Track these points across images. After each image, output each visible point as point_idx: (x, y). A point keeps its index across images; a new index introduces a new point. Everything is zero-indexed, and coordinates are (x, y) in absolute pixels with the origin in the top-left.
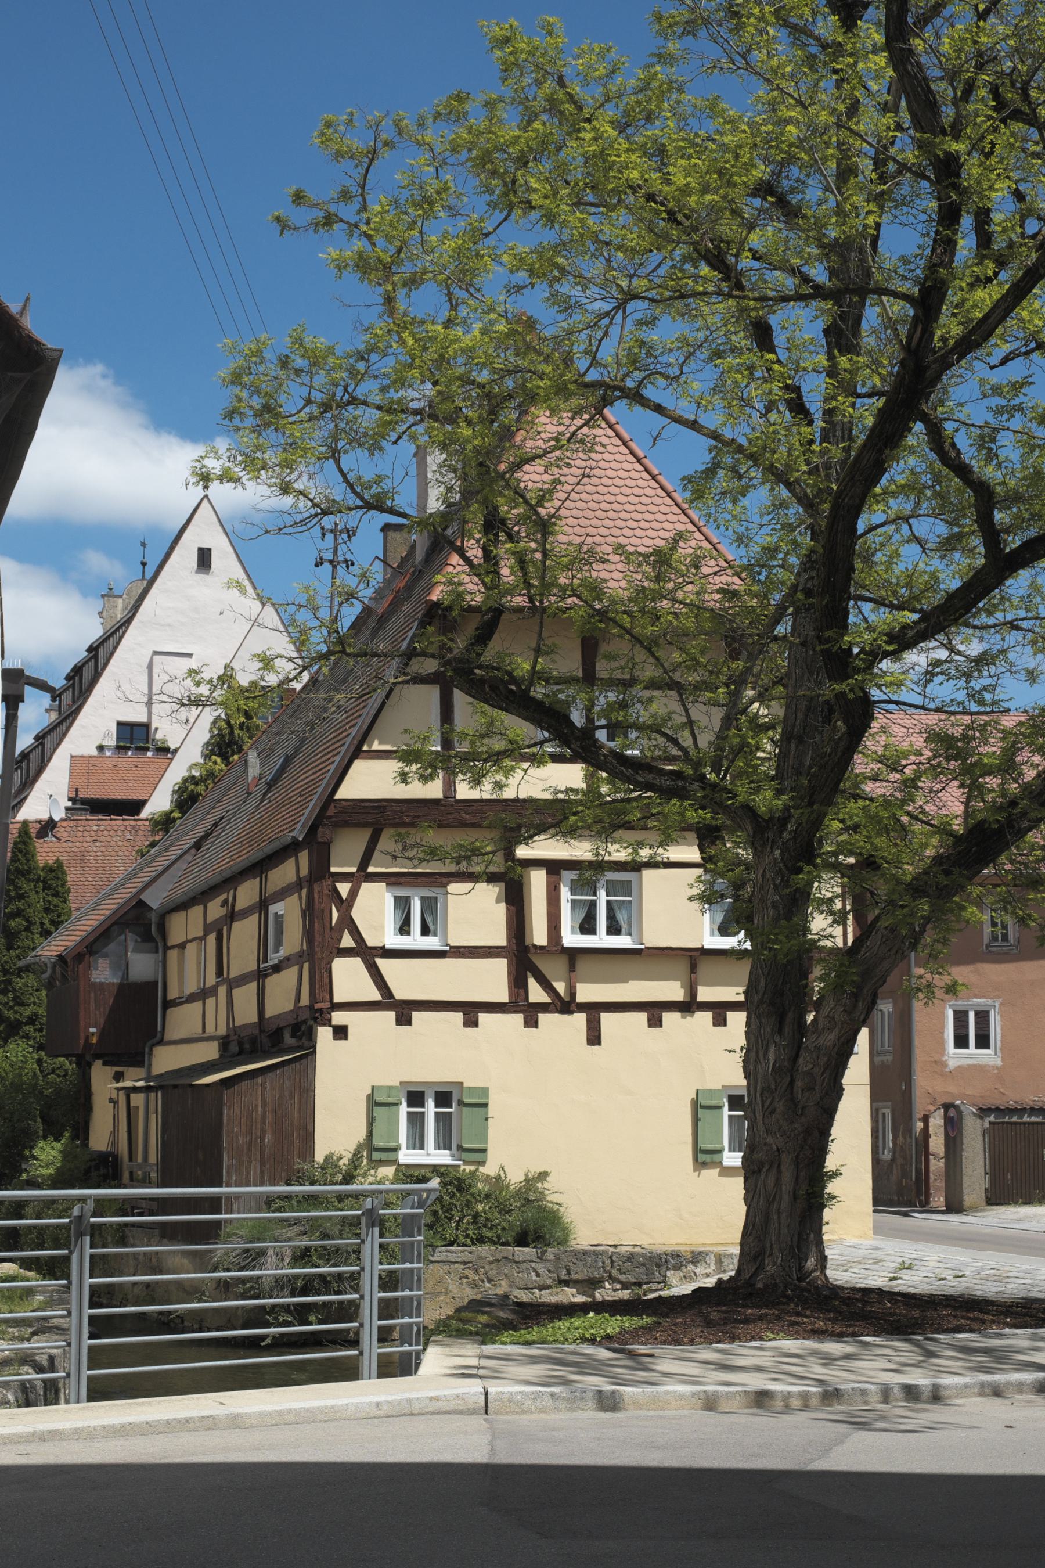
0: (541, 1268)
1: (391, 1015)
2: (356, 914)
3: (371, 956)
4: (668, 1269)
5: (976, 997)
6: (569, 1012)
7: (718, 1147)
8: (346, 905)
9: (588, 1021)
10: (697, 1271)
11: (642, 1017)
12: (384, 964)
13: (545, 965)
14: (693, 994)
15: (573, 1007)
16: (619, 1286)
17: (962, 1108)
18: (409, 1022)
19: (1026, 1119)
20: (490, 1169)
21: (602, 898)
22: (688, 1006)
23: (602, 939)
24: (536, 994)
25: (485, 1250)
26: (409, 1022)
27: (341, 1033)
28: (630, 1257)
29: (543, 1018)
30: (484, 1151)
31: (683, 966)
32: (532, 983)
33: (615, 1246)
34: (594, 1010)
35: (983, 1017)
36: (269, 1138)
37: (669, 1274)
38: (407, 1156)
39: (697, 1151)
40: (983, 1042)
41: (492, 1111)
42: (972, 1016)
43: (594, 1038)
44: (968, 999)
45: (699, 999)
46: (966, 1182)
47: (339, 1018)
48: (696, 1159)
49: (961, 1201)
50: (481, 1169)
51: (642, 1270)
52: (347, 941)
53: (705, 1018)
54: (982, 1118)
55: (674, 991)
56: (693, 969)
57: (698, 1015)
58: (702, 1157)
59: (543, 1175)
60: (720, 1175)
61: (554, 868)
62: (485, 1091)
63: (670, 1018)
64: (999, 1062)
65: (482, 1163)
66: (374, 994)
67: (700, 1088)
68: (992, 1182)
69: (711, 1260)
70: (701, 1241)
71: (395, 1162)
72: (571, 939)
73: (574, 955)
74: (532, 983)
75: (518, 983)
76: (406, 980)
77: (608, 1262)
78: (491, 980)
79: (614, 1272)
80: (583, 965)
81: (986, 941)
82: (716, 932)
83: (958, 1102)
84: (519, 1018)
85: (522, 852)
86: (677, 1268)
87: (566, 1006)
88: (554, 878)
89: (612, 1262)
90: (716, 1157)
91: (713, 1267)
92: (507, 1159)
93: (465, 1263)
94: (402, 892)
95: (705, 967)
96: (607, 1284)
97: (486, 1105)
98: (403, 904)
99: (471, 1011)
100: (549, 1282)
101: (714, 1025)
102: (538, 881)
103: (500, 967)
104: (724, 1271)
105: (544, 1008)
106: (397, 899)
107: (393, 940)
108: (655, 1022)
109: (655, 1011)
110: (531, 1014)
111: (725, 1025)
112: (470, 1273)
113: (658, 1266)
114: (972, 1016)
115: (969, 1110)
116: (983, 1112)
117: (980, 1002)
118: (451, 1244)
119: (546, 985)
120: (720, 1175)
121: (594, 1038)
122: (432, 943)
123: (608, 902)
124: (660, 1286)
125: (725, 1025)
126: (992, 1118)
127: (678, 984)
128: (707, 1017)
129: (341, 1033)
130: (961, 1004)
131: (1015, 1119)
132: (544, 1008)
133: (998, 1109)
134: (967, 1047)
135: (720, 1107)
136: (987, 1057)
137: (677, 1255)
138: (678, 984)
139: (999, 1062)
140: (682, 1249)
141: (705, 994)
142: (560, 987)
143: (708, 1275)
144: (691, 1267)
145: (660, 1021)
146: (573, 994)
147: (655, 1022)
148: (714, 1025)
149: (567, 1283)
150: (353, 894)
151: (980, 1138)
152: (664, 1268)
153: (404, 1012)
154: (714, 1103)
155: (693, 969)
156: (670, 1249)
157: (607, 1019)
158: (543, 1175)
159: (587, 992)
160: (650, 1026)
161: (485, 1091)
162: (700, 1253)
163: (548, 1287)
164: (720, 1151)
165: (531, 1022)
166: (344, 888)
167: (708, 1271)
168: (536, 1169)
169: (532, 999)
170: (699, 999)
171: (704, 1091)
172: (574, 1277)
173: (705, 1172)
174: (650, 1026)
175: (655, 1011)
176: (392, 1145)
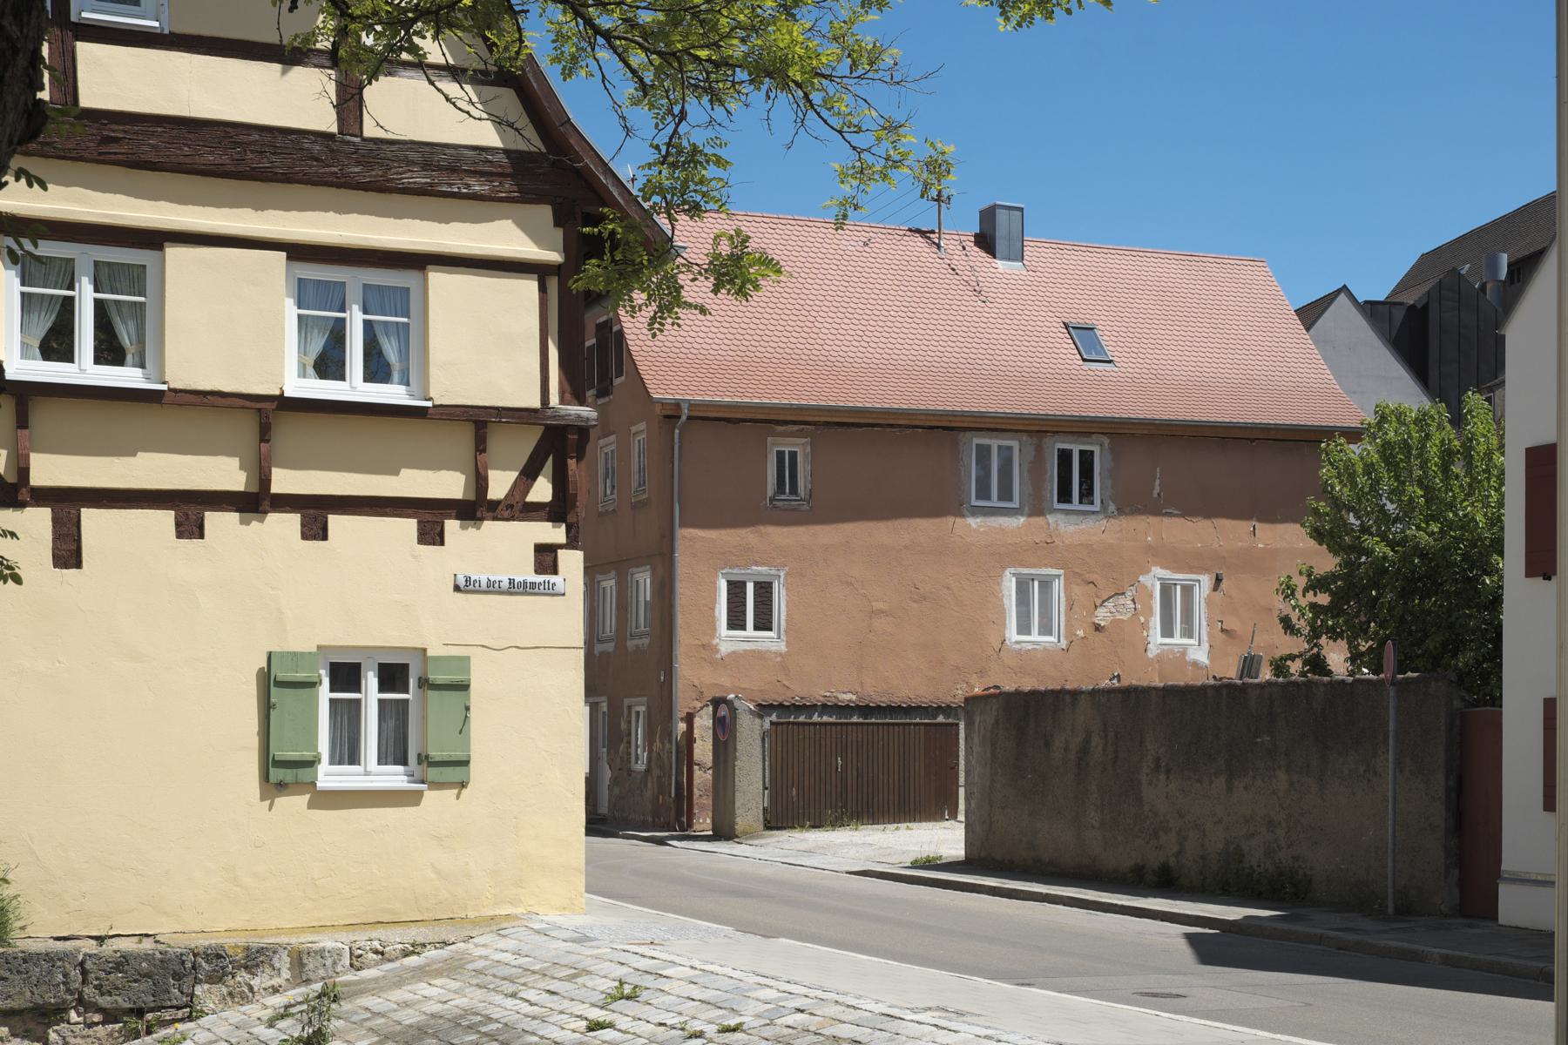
4: (197, 981)
5: (756, 563)
6: (20, 505)
7: (307, 755)
10: (255, 982)
11: (165, 519)
14: (265, 481)
16: (97, 1018)
17: (737, 704)
19: (816, 718)
21: (86, 296)
22: (254, 502)
28: (122, 962)
31: (246, 427)
33: (100, 939)
35: (764, 590)
37: (198, 990)
40: (763, 623)
42: (750, 588)
44: (746, 566)
45: (275, 489)
46: (739, 800)
48: (265, 776)
49: (732, 824)
51: (146, 985)
53: (288, 524)
54: (761, 717)
55: (228, 474)
56: (265, 433)
57: (273, 518)
58: (276, 774)
60: (311, 806)
63: (219, 522)
64: (782, 647)
67: (275, 648)
68: (774, 799)
69: (283, 962)
70: (274, 924)
77: (76, 974)
79: (89, 991)
81: (770, 493)
82: (310, 370)
83: (731, 696)
86: (216, 978)
89: (84, 973)
90: (303, 774)
91: (286, 974)
95: (288, 431)
96: (73, 1015)
101: (305, 537)
104: (308, 981)
108: (190, 528)
109: (190, 510)
111: (325, 538)
113: (178, 976)
114: (750, 588)
115: (745, 706)
116: (764, 709)
117: (762, 570)
120: (311, 806)
123: (99, 304)
124: (180, 1014)
125: (325, 538)
126: (774, 718)
127: (234, 462)
130: (737, 574)
131: (802, 719)
133: (781, 706)
134: (743, 627)
135: (313, 685)
136: (769, 641)
137: (216, 955)
138: (234, 462)
139: (782, 647)
140: (228, 941)
141: (284, 481)
143: (275, 990)
144: (242, 976)
145: (201, 527)
147: (190, 528)
148: (305, 537)
151: (759, 742)
152: (189, 980)
154: (301, 676)
155: (265, 433)
156: (202, 942)
157: (92, 520)
160: (180, 535)
162: (260, 951)
164: (311, 764)
167: (276, 982)
170: (275, 489)
171: (282, 655)
173: (283, 802)
174: (180, 535)
175: (190, 510)
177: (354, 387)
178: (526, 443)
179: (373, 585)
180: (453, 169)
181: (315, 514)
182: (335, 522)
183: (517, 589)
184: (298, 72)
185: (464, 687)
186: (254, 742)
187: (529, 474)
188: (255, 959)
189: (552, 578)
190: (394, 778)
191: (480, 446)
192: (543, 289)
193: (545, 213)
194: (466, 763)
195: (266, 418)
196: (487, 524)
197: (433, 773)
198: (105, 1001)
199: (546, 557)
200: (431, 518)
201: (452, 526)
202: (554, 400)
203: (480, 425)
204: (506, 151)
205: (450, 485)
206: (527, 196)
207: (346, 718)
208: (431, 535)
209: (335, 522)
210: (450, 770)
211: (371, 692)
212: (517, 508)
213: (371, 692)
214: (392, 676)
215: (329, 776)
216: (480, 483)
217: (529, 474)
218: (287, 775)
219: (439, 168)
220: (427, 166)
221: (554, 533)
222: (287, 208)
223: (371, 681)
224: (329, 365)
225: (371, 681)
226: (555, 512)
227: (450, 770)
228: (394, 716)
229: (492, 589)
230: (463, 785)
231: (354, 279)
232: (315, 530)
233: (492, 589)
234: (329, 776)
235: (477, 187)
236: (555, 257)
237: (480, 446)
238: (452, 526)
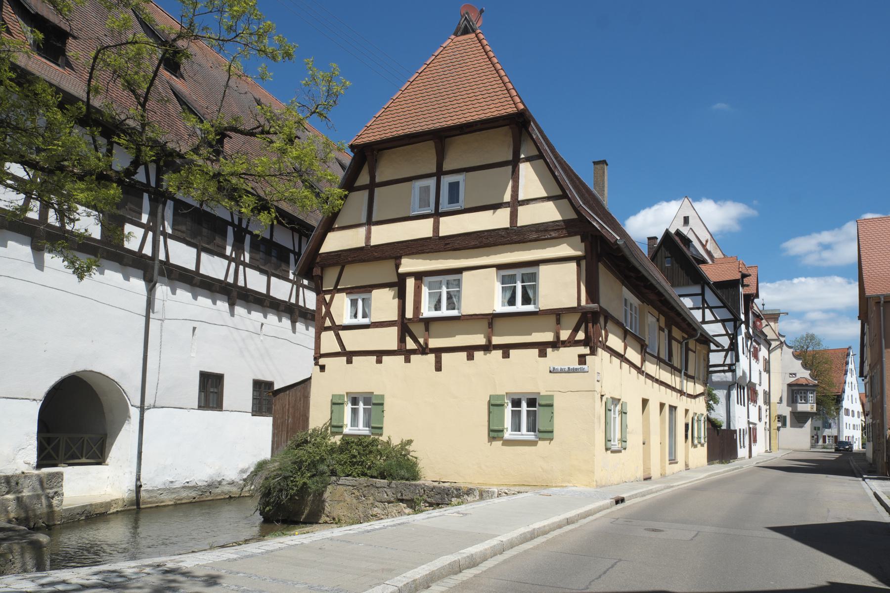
0: (388, 491)
1: (345, 359)
2: (332, 310)
3: (337, 329)
6: (427, 354)
8: (328, 305)
9: (436, 357)
10: (469, 499)
11: (464, 354)
12: (341, 333)
13: (414, 328)
14: (489, 341)
15: (427, 351)
18: (351, 363)
20: (384, 438)
22: (487, 348)
23: (444, 312)
24: (410, 344)
25: (362, 480)
26: (351, 363)
27: (322, 368)
29: (413, 357)
30: (381, 428)
32: (409, 340)
34: (438, 352)
36: (290, 420)
38: (347, 430)
39: (491, 431)
41: (386, 407)
43: (438, 368)
47: (322, 361)
50: (381, 438)
52: (328, 323)
53: (499, 353)
55: (480, 340)
57: (494, 352)
58: (492, 434)
59: (410, 442)
61: (419, 276)
62: (382, 397)
63: (478, 355)
65: (381, 435)
66: (339, 350)
69: (477, 493)
71: (341, 433)
72: (427, 312)
73: (428, 322)
74: (409, 340)
75: (402, 340)
76: (353, 340)
78: (389, 338)
80: (433, 327)
84: (402, 358)
85: (402, 270)
86: (458, 496)
87: (424, 350)
88: (419, 282)
90: (500, 434)
92: (393, 433)
93: (353, 486)
94: (354, 297)
95: (498, 324)
97: (382, 404)
98: (354, 303)
99: (379, 355)
100: (392, 499)
102: (410, 283)
103: (394, 331)
105: (413, 352)
106: (352, 300)
107: (347, 320)
108: (470, 357)
109: (470, 351)
110: (407, 354)
112: (355, 491)
113: (447, 495)
118: (348, 476)
119: (415, 340)
121: (438, 368)
122: (366, 321)
127: (482, 336)
128: (499, 353)
129: (322, 368)
132: (413, 352)
137: (458, 489)
138: (482, 336)
141: (496, 340)
142: (421, 341)
144: (466, 497)
146: (426, 344)
147: (470, 357)
149: (402, 501)
150: (332, 299)
153: (350, 356)
154: (499, 402)
157: (445, 356)
158: (410, 442)
159: (434, 343)
161: (382, 397)
162: (471, 489)
163: (392, 502)
165: (408, 360)
166: (328, 297)
168: (406, 438)
169: (408, 348)
172: (404, 497)
173: (494, 443)
176: (340, 424)
177: (519, 307)
178: (575, 319)
179: (525, 372)
180: (546, 231)
181: (506, 349)
182: (512, 352)
183: (575, 371)
184: (499, 210)
185: (551, 405)
186: (487, 424)
187: (576, 330)
188: (469, 492)
189: (583, 366)
190: (531, 436)
191: (558, 322)
192: (579, 265)
193: (578, 238)
194: (552, 432)
195: (491, 320)
196: (562, 349)
197: (541, 435)
198: (429, 500)
199: (582, 359)
200: (542, 348)
201: (549, 350)
202: (583, 303)
203: (558, 315)
204: (563, 221)
205: (549, 337)
206: (570, 234)
207: (516, 415)
208: (543, 354)
209: (512, 352)
210: (547, 434)
211: (524, 407)
212: (572, 342)
213: (524, 407)
214: (532, 402)
215: (508, 434)
216: (557, 336)
217: (576, 330)
218: (495, 434)
219: (541, 231)
220: (537, 231)
221: (586, 350)
222: (500, 253)
223: (524, 404)
224: (512, 302)
225: (524, 404)
226: (585, 343)
227: (547, 434)
228: (532, 416)
229: (562, 371)
230: (551, 439)
231: (519, 272)
232: (506, 355)
233: (562, 371)
234: (516, 436)
235: (553, 234)
236: (579, 253)
237: (558, 322)
238: (549, 350)
